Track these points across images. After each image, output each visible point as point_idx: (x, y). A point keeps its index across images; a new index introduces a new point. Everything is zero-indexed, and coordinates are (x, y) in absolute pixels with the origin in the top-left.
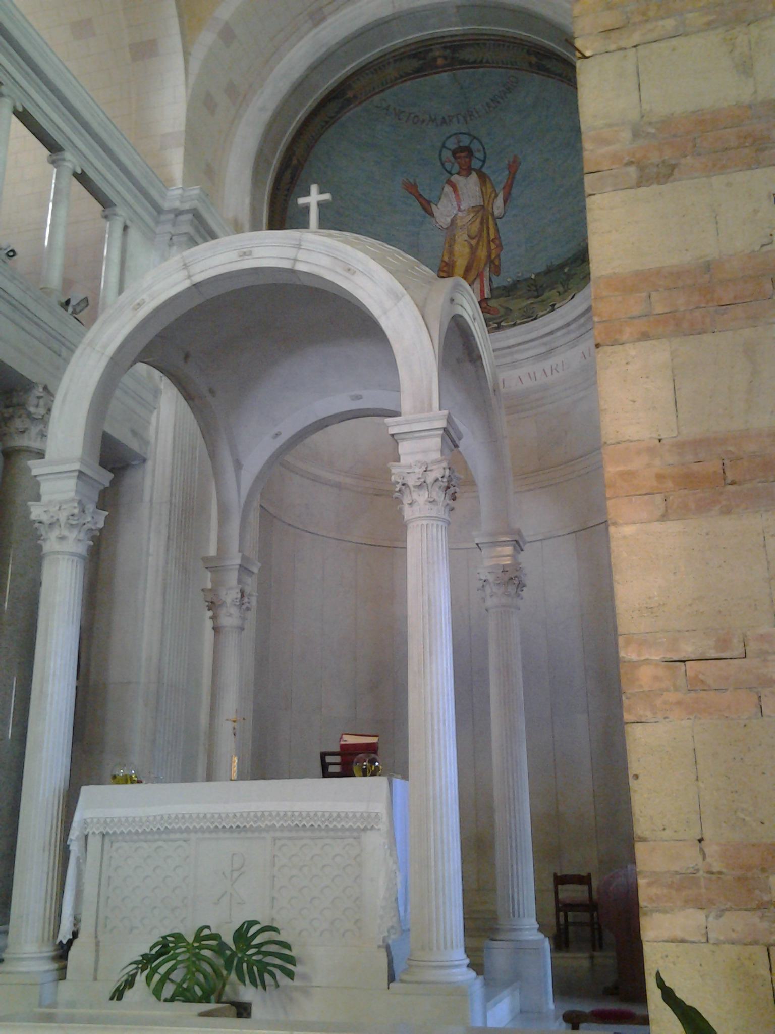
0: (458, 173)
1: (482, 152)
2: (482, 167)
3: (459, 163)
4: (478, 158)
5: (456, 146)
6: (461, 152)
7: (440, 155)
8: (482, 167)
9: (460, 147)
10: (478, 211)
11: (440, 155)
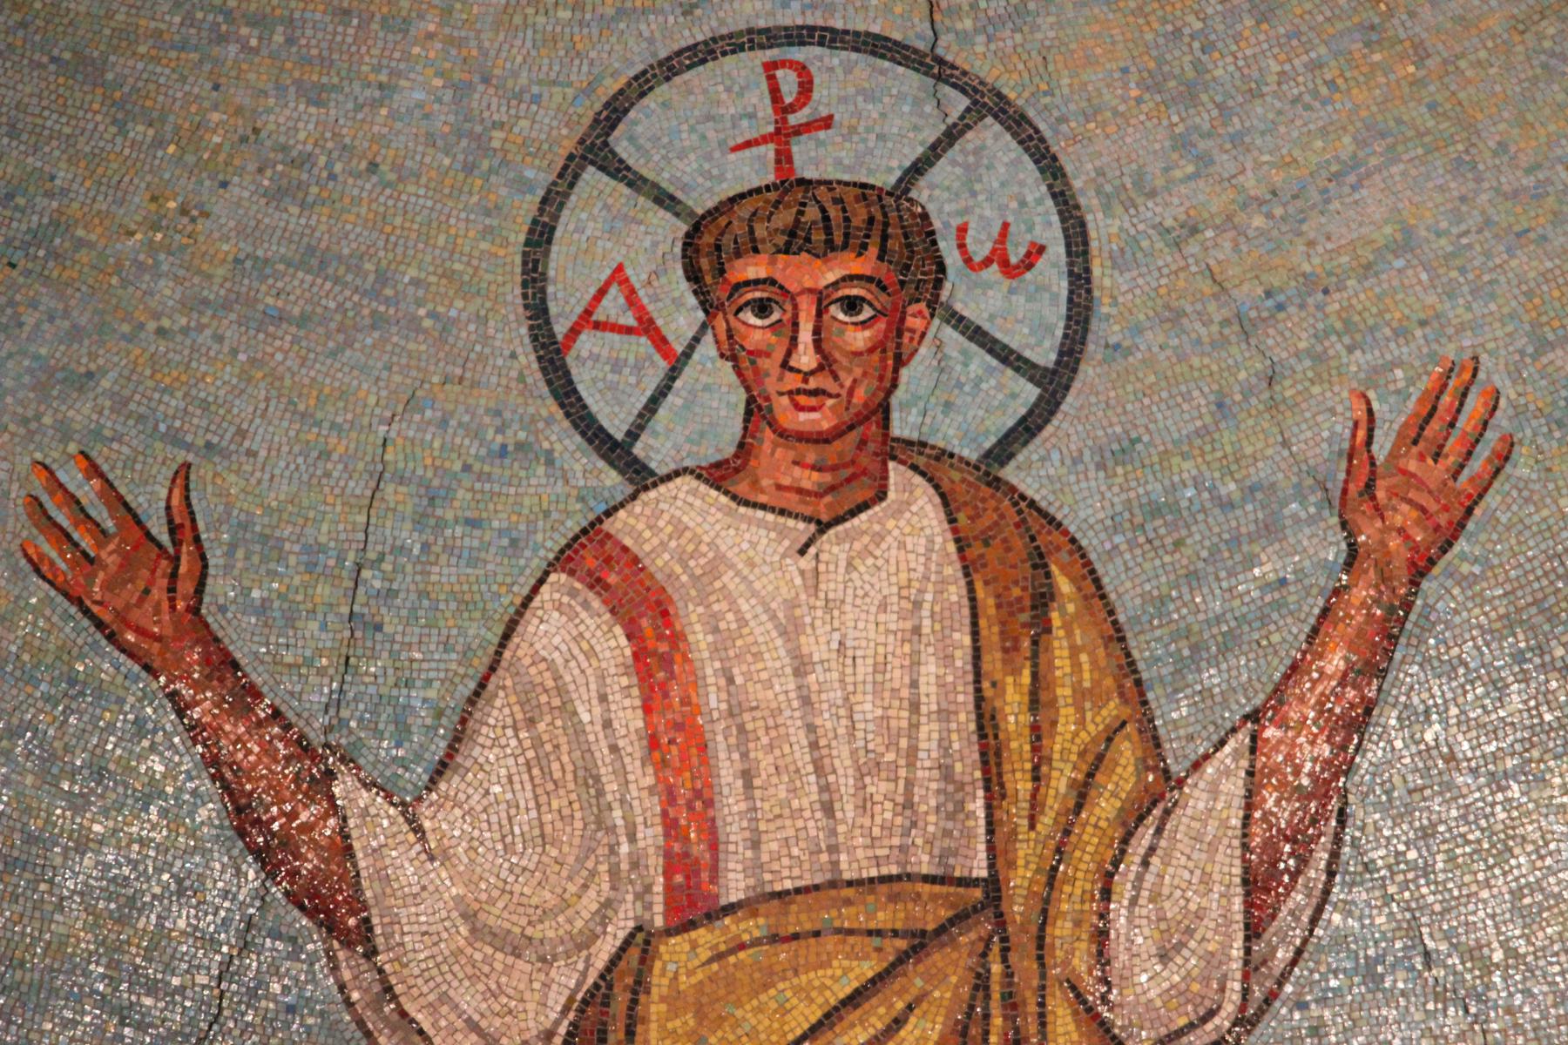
0: (718, 475)
1: (1052, 272)
2: (1028, 428)
3: (732, 352)
4: (977, 335)
5: (756, 169)
6: (794, 241)
7: (541, 236)
8: (1028, 428)
9: (789, 185)
10: (920, 943)
11: (541, 236)
